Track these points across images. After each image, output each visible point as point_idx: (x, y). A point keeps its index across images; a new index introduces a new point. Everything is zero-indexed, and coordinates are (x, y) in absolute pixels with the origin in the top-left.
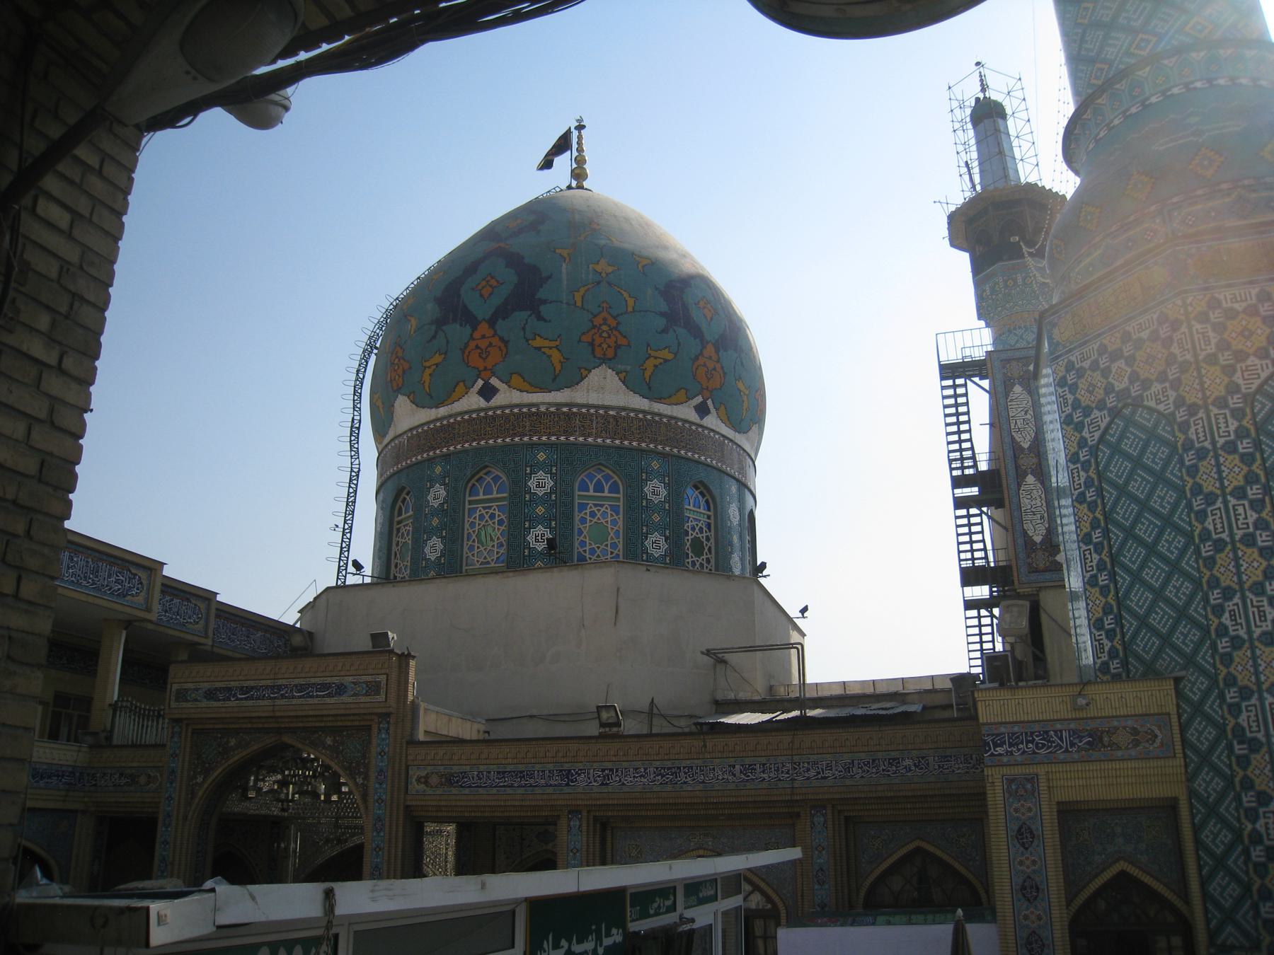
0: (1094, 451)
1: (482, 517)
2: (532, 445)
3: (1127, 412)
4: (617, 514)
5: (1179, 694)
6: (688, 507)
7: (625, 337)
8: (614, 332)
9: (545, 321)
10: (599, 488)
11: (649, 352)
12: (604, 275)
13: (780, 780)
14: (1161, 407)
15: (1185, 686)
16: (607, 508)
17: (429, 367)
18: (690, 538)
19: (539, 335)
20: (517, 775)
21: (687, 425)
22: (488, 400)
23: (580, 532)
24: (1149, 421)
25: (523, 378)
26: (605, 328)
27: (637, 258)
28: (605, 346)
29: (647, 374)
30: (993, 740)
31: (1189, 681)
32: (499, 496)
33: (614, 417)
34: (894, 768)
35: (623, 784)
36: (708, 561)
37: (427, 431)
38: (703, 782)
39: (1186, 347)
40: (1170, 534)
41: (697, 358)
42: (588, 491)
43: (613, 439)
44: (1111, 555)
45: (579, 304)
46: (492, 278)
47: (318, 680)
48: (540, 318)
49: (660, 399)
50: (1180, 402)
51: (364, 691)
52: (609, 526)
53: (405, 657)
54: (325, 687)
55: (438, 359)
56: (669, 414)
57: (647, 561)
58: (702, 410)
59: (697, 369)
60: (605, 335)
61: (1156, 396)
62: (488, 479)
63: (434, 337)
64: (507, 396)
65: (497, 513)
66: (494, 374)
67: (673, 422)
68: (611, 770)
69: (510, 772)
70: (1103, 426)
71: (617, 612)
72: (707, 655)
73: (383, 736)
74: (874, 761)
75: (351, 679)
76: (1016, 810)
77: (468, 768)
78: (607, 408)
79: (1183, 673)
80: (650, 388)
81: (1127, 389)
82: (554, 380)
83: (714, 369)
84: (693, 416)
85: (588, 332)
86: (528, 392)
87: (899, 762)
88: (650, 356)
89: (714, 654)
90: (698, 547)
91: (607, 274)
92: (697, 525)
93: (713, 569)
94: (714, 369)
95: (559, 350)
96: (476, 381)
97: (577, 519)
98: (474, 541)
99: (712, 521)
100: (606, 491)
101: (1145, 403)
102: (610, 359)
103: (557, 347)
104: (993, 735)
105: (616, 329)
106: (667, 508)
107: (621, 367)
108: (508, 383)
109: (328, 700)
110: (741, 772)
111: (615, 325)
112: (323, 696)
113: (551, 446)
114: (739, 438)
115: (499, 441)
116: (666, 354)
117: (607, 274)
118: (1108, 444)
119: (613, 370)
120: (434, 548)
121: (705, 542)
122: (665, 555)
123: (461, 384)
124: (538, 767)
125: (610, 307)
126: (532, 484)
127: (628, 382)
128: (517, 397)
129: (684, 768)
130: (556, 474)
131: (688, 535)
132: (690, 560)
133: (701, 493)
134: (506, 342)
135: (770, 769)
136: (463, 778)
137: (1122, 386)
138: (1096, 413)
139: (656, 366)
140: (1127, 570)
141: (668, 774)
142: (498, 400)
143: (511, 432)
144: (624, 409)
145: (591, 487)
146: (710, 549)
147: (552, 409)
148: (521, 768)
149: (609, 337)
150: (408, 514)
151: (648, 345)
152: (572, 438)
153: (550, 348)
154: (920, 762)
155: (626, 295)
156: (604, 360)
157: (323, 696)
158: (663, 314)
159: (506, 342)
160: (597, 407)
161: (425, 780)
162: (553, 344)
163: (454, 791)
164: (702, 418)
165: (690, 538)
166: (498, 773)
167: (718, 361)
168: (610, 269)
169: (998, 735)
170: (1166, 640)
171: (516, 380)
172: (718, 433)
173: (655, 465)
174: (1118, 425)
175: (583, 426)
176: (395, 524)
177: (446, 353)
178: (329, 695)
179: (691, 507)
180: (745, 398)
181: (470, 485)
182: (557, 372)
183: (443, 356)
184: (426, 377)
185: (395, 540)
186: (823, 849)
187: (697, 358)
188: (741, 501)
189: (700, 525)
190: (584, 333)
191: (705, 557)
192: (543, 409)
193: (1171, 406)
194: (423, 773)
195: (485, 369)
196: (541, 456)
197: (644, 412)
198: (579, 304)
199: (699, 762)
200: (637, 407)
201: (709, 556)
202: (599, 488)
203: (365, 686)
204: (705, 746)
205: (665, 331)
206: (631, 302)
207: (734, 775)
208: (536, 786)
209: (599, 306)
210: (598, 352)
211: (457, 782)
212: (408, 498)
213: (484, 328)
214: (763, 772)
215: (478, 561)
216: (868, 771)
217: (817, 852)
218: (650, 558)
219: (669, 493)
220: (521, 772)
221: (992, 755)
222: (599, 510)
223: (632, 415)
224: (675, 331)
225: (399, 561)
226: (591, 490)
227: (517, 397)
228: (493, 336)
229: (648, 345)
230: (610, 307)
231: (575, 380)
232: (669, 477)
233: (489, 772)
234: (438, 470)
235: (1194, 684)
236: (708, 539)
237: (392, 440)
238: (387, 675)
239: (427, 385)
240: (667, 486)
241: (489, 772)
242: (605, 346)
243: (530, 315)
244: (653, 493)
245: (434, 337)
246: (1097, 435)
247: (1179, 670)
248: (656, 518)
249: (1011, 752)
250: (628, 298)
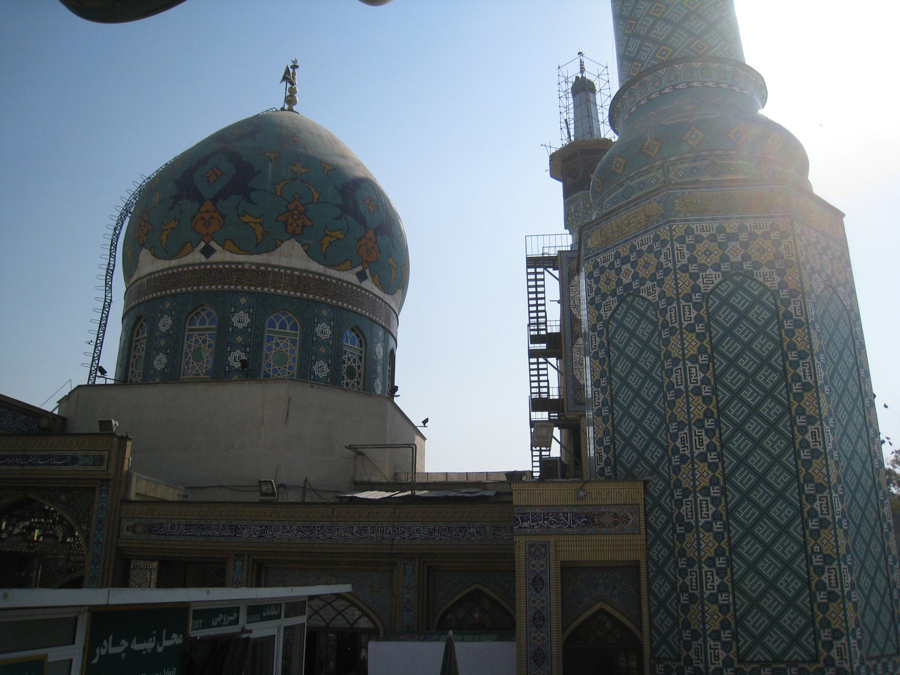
0: (607, 324)
1: (196, 341)
2: (237, 292)
3: (629, 299)
4: (295, 345)
5: (646, 491)
6: (346, 344)
7: (310, 220)
8: (302, 216)
9: (253, 203)
10: (283, 326)
12: (299, 174)
13: (384, 539)
14: (651, 298)
15: (650, 486)
16: (287, 341)
17: (166, 230)
18: (346, 365)
19: (248, 213)
20: (199, 527)
21: (350, 286)
22: (207, 257)
23: (267, 357)
24: (642, 306)
25: (234, 243)
26: (296, 212)
27: (324, 165)
28: (295, 225)
29: (324, 248)
30: (521, 518)
31: (653, 483)
32: (210, 327)
33: (297, 276)
34: (463, 534)
35: (275, 537)
36: (358, 383)
37: (161, 276)
38: (331, 538)
39: (669, 259)
40: (649, 384)
41: (361, 239)
42: (275, 328)
43: (296, 292)
44: (611, 396)
45: (279, 193)
46: (218, 169)
47: (58, 453)
48: (250, 201)
49: (331, 266)
50: (662, 295)
51: (91, 463)
52: (289, 354)
53: (124, 439)
54: (63, 458)
55: (173, 224)
56: (338, 277)
57: (314, 381)
58: (362, 276)
59: (360, 246)
60: (295, 217)
61: (648, 290)
62: (203, 314)
63: (172, 208)
64: (221, 256)
65: (208, 339)
66: (213, 239)
67: (340, 283)
68: (267, 527)
69: (194, 525)
70: (613, 307)
71: (287, 415)
72: (350, 449)
73: (104, 496)
74: (449, 528)
75: (82, 453)
76: (533, 566)
77: (164, 521)
78: (293, 269)
79: (648, 478)
80: (325, 258)
81: (631, 284)
82: (256, 246)
83: (373, 248)
84: (355, 280)
85: (283, 214)
86: (237, 254)
87: (466, 530)
88: (327, 235)
89: (354, 448)
90: (351, 373)
91: (301, 174)
92: (352, 357)
93: (361, 389)
94: (373, 248)
95: (262, 226)
96: (199, 243)
97: (265, 347)
98: (190, 358)
99: (363, 355)
100: (288, 328)
101: (641, 294)
102: (297, 235)
103: (260, 223)
104: (521, 514)
105: (304, 213)
106: (331, 343)
108: (223, 246)
109: (64, 468)
110: (357, 532)
111: (303, 211)
112: (61, 465)
113: (251, 293)
114: (387, 298)
115: (213, 287)
116: (338, 234)
117: (301, 174)
118: (615, 320)
119: (299, 243)
120: (160, 361)
121: (357, 370)
122: (327, 377)
123: (189, 244)
124: (215, 522)
125: (301, 198)
126: (235, 320)
127: (310, 252)
128: (229, 257)
129: (318, 527)
130: (252, 314)
131: (345, 364)
132: (345, 382)
133: (357, 335)
134: (223, 217)
135: (378, 530)
136: (160, 528)
137: (628, 281)
138: (610, 298)
140: (620, 406)
141: (306, 531)
142: (215, 257)
143: (222, 281)
144: (305, 271)
145: (277, 325)
146: (360, 375)
147: (254, 267)
148: (203, 522)
149: (298, 219)
150: (143, 336)
151: (326, 227)
152: (266, 289)
153: (256, 223)
154: (480, 530)
155: (313, 190)
156: (293, 235)
157: (61, 465)
158: (338, 206)
159: (223, 217)
160: (286, 268)
161: (132, 529)
162: (257, 220)
163: (154, 537)
164: (361, 282)
165: (346, 365)
166: (186, 525)
167: (376, 242)
168: (303, 171)
169: (525, 514)
170: (641, 455)
171: (229, 244)
172: (372, 293)
173: (325, 313)
174: (623, 308)
175: (275, 281)
176: (134, 342)
177: (179, 221)
178: (65, 464)
179: (349, 344)
180: (394, 271)
181: (190, 317)
182: (259, 240)
183: (177, 223)
184: (164, 237)
185: (133, 353)
186: (411, 588)
187: (361, 239)
188: (386, 343)
189: (354, 357)
190: (280, 215)
191: (356, 380)
192: (246, 267)
193: (657, 297)
194: (131, 524)
195: (207, 234)
196: (243, 300)
197: (320, 274)
198: (279, 193)
199: (329, 524)
200: (315, 270)
201: (359, 379)
202: (283, 326)
203: (92, 458)
204: (333, 512)
205: (339, 218)
206: (316, 195)
207: (353, 534)
208: (212, 536)
209: (293, 196)
210: (290, 229)
211: (157, 530)
212: (144, 324)
213: (208, 205)
214: (373, 532)
215: (191, 373)
216: (445, 535)
217: (406, 590)
218: (316, 379)
219: (333, 333)
220: (203, 525)
221: (520, 527)
222: (282, 342)
223: (311, 275)
224: (346, 218)
225: (135, 370)
226: (277, 327)
227: (229, 257)
228: (215, 211)
229: (326, 227)
231: (271, 248)
232: (334, 321)
233: (179, 525)
234: (168, 305)
235: (655, 485)
236: (359, 367)
237: (136, 281)
238: (109, 451)
239: (164, 242)
240: (332, 328)
241: (179, 525)
242: (295, 225)
243: (242, 199)
244: (322, 332)
245: (172, 208)
246: (609, 313)
247: (647, 476)
248: (322, 350)
249: (533, 526)
250: (314, 192)
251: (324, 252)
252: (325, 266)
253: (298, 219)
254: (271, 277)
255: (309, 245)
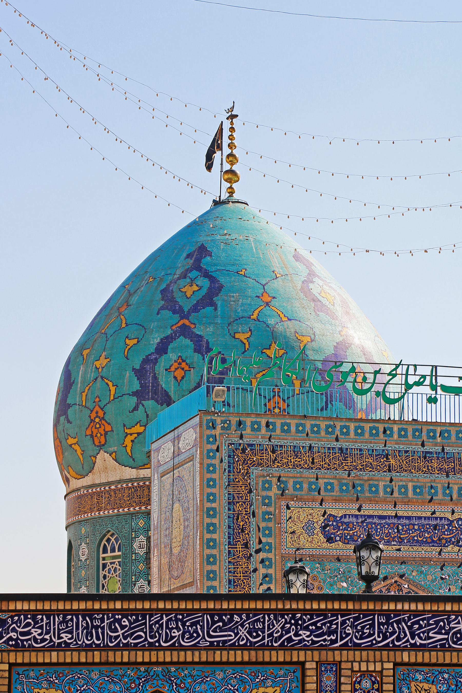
7: (109, 424)
11: (126, 431)
26: (97, 420)
88: (127, 434)
102: (103, 445)
107: (112, 449)
139: (132, 441)
205: (136, 409)
209: (94, 402)
224: (143, 406)
229: (124, 426)
230: (100, 401)
251: (130, 454)
252: (137, 468)
253: (100, 427)
254: (95, 500)
255: (115, 452)
